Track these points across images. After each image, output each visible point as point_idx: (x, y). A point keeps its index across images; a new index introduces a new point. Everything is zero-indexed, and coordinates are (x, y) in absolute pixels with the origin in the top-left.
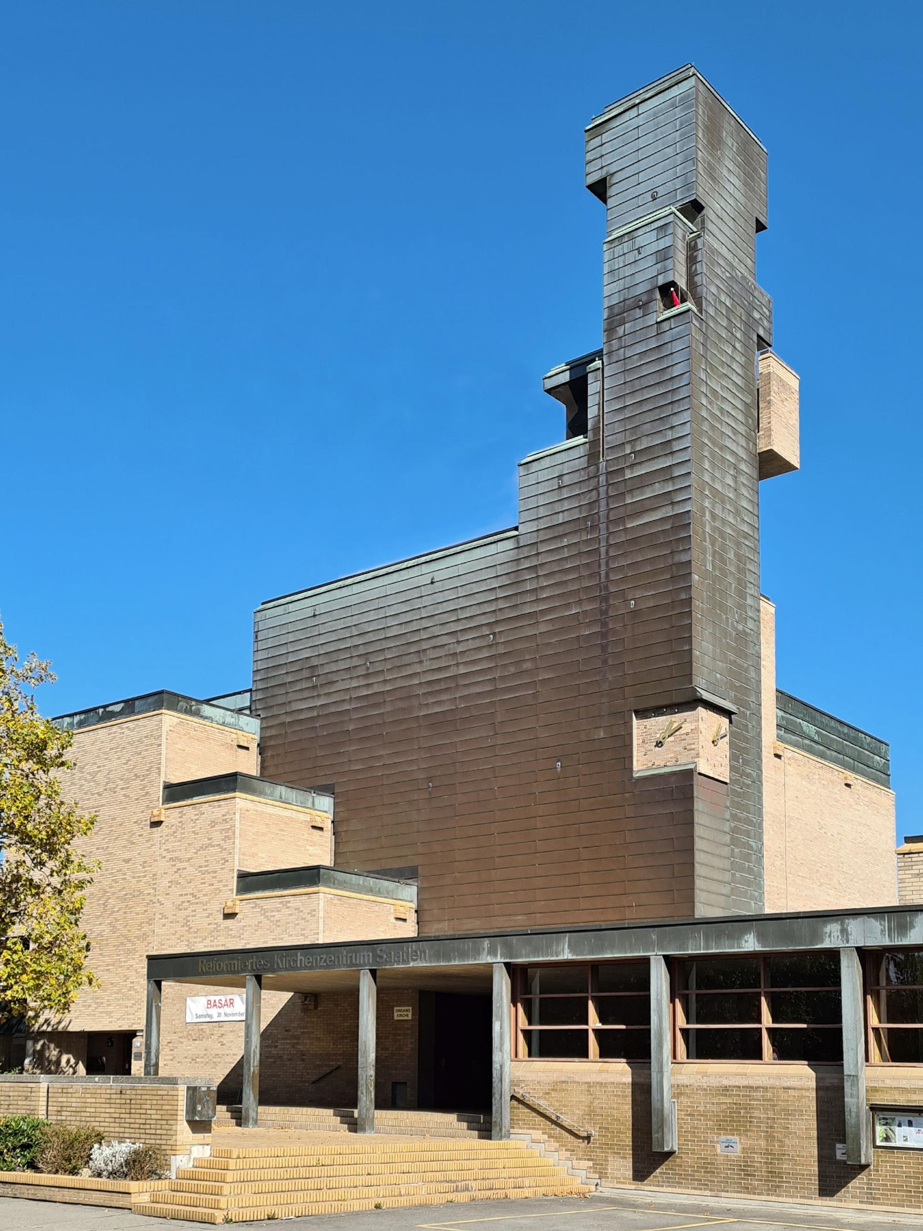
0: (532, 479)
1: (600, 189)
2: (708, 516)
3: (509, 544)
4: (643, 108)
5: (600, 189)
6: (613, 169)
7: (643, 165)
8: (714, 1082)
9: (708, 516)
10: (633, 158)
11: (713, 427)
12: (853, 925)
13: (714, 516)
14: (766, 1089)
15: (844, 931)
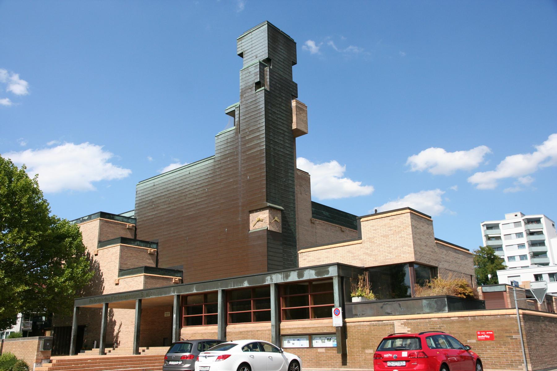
0: (219, 141)
1: (241, 55)
2: (272, 149)
3: (212, 161)
4: (253, 33)
5: (241, 55)
6: (245, 50)
7: (253, 48)
8: (237, 330)
9: (272, 149)
10: (251, 47)
11: (274, 123)
14: (252, 331)
15: (271, 279)
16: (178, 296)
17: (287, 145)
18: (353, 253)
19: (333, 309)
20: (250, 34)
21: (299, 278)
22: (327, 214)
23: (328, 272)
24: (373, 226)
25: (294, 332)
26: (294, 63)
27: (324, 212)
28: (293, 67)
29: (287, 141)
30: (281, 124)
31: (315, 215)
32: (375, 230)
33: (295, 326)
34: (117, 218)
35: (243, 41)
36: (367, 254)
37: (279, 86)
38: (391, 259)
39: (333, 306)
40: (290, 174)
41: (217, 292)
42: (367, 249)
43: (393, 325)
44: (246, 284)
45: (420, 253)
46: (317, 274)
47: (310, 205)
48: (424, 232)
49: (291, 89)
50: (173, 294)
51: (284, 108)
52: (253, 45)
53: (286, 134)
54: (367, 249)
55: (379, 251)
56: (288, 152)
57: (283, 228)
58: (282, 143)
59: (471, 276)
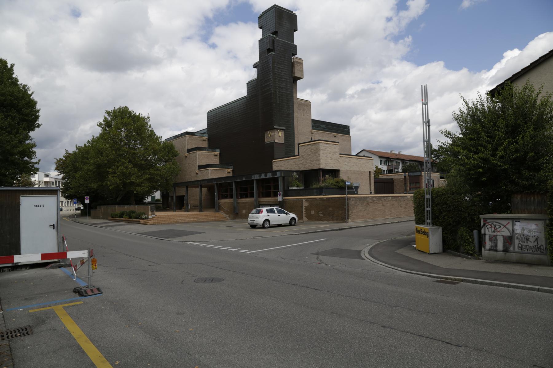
13: (279, 92)
16: (217, 184)
22: (324, 126)
23: (276, 174)
25: (264, 203)
26: (296, 30)
27: (321, 126)
28: (295, 33)
34: (196, 134)
44: (244, 179)
47: (310, 122)
57: (285, 140)
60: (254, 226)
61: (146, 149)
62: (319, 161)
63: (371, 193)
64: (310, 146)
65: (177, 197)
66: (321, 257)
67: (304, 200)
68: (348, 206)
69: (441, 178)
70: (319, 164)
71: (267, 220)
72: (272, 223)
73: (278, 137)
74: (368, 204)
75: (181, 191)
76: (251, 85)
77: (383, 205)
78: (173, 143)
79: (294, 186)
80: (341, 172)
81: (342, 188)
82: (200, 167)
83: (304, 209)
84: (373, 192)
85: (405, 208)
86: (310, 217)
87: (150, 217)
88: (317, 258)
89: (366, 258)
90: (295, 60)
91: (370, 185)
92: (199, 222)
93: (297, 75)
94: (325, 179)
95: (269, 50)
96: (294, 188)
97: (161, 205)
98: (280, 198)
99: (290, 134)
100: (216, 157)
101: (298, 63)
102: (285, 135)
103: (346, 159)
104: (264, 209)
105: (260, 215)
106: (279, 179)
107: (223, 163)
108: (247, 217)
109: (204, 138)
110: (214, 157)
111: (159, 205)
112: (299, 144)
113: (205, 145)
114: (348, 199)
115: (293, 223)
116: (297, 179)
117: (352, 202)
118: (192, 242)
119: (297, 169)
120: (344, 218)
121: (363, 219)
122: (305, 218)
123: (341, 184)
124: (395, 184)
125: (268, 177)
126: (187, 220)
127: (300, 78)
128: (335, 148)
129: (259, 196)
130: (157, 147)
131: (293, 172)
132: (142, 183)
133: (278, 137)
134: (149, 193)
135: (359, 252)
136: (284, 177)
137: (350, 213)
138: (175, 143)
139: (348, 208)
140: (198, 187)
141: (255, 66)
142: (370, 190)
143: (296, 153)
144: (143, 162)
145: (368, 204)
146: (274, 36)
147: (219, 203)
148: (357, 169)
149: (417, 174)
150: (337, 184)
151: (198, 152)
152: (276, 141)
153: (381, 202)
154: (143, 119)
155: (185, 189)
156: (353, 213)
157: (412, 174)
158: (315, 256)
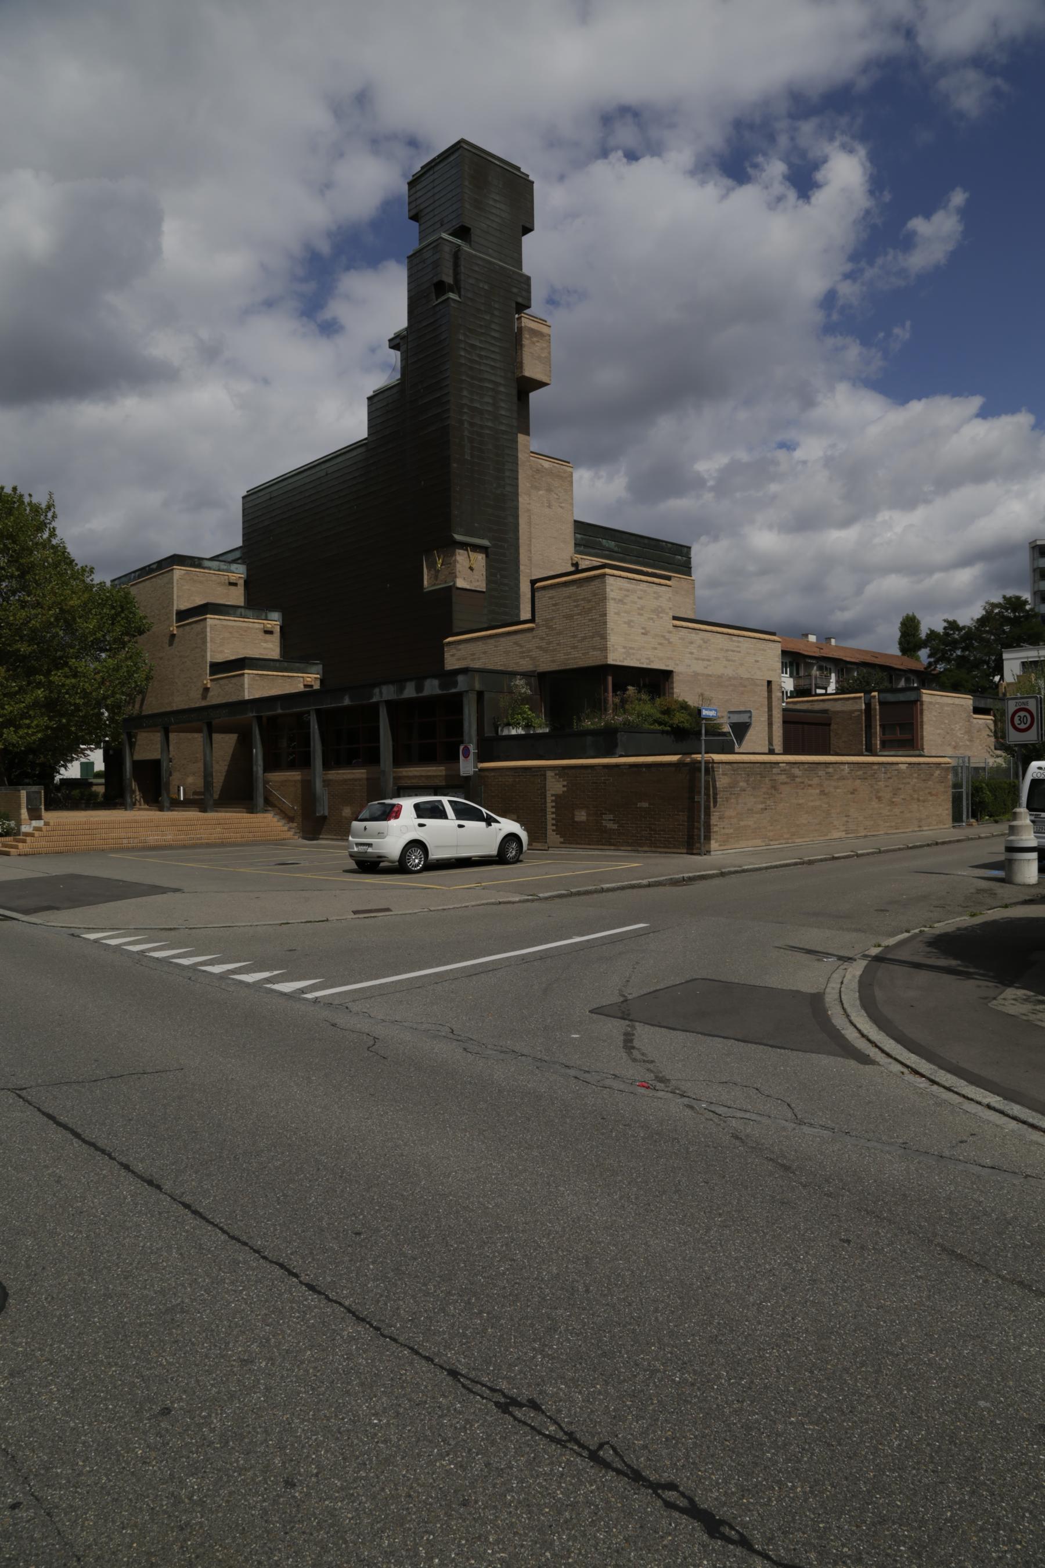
2: (466, 425)
6: (422, 207)
9: (466, 425)
12: (384, 689)
13: (472, 424)
15: (381, 692)
16: (259, 718)
17: (503, 412)
18: (521, 646)
19: (461, 748)
20: (431, 172)
21: (417, 692)
24: (550, 598)
25: (415, 782)
26: (527, 230)
28: (527, 240)
29: (503, 405)
30: (488, 369)
31: (582, 548)
32: (555, 605)
33: (416, 774)
34: (207, 563)
35: (418, 187)
36: (540, 648)
37: (486, 287)
38: (575, 658)
39: (462, 742)
40: (507, 474)
41: (308, 712)
42: (542, 639)
43: (545, 775)
44: (347, 702)
45: (624, 647)
46: (442, 686)
47: (569, 529)
48: (642, 608)
49: (515, 290)
50: (251, 715)
51: (496, 335)
52: (437, 197)
53: (502, 389)
54: (542, 639)
55: (558, 644)
56: (503, 428)
57: (489, 581)
58: (490, 409)
59: (769, 683)
60: (369, 865)
61: (38, 605)
62: (604, 637)
63: (771, 752)
64: (573, 589)
65: (137, 765)
66: (646, 1036)
67: (550, 774)
68: (707, 795)
69: (977, 710)
70: (604, 649)
71: (416, 844)
72: (435, 855)
73: (469, 571)
74: (774, 788)
75: (147, 747)
76: (381, 406)
77: (823, 793)
78: (133, 591)
79: (516, 725)
80: (676, 678)
81: (688, 730)
82: (217, 668)
83: (550, 804)
84: (778, 747)
85: (892, 803)
86: (575, 835)
87: (25, 829)
88: (628, 1043)
89: (872, 1052)
90: (526, 322)
91: (770, 724)
92: (194, 846)
93: (532, 370)
94: (624, 702)
95: (440, 288)
96: (514, 732)
97: (101, 790)
98: (467, 767)
99: (503, 559)
100: (268, 636)
101: (534, 333)
102: (489, 566)
103: (693, 636)
104: (407, 804)
105: (393, 823)
106: (465, 701)
107: (293, 654)
108: (344, 831)
109: (233, 578)
110: (261, 635)
111: (94, 788)
112: (533, 582)
113: (236, 597)
114: (710, 768)
115: (512, 853)
116: (526, 700)
117: (722, 781)
118: (111, 933)
119: (525, 665)
120: (693, 838)
121: (758, 842)
122: (553, 837)
123: (680, 718)
124: (833, 727)
125: (426, 692)
126: (153, 839)
127: (541, 385)
128: (658, 597)
129: (398, 762)
130: (75, 602)
131: (513, 674)
132: (24, 715)
133: (469, 571)
134: (66, 754)
135: (816, 1000)
136: (480, 695)
137: (714, 820)
138: (141, 593)
139: (708, 801)
140: (199, 731)
141: (395, 343)
142: (770, 743)
143: (525, 614)
144: (24, 648)
145: (774, 788)
146: (459, 242)
147: (266, 782)
148: (729, 672)
149: (910, 696)
150: (666, 718)
151: (212, 620)
152: (460, 583)
153: (815, 781)
154: (36, 509)
155: (158, 737)
156: (725, 819)
157: (890, 697)
158: (615, 1028)
